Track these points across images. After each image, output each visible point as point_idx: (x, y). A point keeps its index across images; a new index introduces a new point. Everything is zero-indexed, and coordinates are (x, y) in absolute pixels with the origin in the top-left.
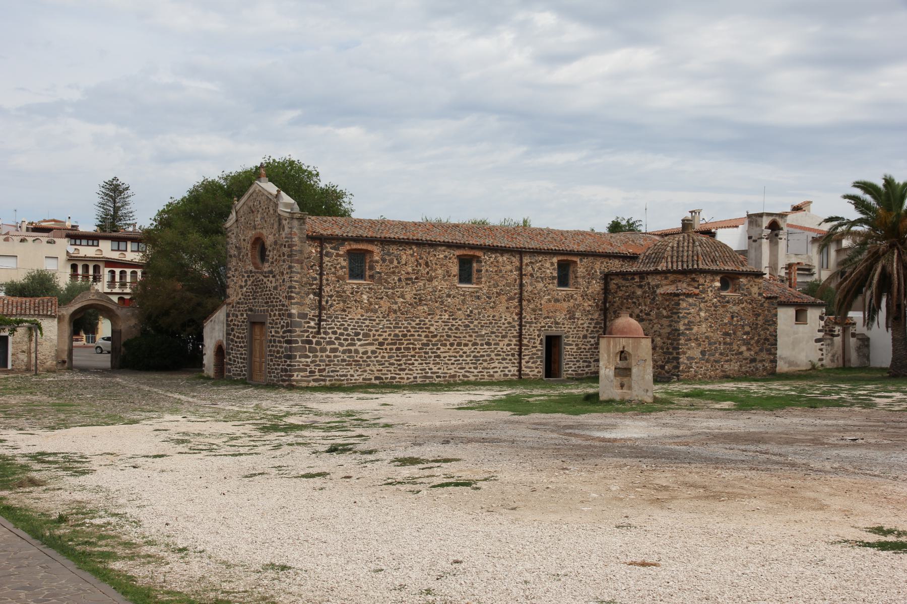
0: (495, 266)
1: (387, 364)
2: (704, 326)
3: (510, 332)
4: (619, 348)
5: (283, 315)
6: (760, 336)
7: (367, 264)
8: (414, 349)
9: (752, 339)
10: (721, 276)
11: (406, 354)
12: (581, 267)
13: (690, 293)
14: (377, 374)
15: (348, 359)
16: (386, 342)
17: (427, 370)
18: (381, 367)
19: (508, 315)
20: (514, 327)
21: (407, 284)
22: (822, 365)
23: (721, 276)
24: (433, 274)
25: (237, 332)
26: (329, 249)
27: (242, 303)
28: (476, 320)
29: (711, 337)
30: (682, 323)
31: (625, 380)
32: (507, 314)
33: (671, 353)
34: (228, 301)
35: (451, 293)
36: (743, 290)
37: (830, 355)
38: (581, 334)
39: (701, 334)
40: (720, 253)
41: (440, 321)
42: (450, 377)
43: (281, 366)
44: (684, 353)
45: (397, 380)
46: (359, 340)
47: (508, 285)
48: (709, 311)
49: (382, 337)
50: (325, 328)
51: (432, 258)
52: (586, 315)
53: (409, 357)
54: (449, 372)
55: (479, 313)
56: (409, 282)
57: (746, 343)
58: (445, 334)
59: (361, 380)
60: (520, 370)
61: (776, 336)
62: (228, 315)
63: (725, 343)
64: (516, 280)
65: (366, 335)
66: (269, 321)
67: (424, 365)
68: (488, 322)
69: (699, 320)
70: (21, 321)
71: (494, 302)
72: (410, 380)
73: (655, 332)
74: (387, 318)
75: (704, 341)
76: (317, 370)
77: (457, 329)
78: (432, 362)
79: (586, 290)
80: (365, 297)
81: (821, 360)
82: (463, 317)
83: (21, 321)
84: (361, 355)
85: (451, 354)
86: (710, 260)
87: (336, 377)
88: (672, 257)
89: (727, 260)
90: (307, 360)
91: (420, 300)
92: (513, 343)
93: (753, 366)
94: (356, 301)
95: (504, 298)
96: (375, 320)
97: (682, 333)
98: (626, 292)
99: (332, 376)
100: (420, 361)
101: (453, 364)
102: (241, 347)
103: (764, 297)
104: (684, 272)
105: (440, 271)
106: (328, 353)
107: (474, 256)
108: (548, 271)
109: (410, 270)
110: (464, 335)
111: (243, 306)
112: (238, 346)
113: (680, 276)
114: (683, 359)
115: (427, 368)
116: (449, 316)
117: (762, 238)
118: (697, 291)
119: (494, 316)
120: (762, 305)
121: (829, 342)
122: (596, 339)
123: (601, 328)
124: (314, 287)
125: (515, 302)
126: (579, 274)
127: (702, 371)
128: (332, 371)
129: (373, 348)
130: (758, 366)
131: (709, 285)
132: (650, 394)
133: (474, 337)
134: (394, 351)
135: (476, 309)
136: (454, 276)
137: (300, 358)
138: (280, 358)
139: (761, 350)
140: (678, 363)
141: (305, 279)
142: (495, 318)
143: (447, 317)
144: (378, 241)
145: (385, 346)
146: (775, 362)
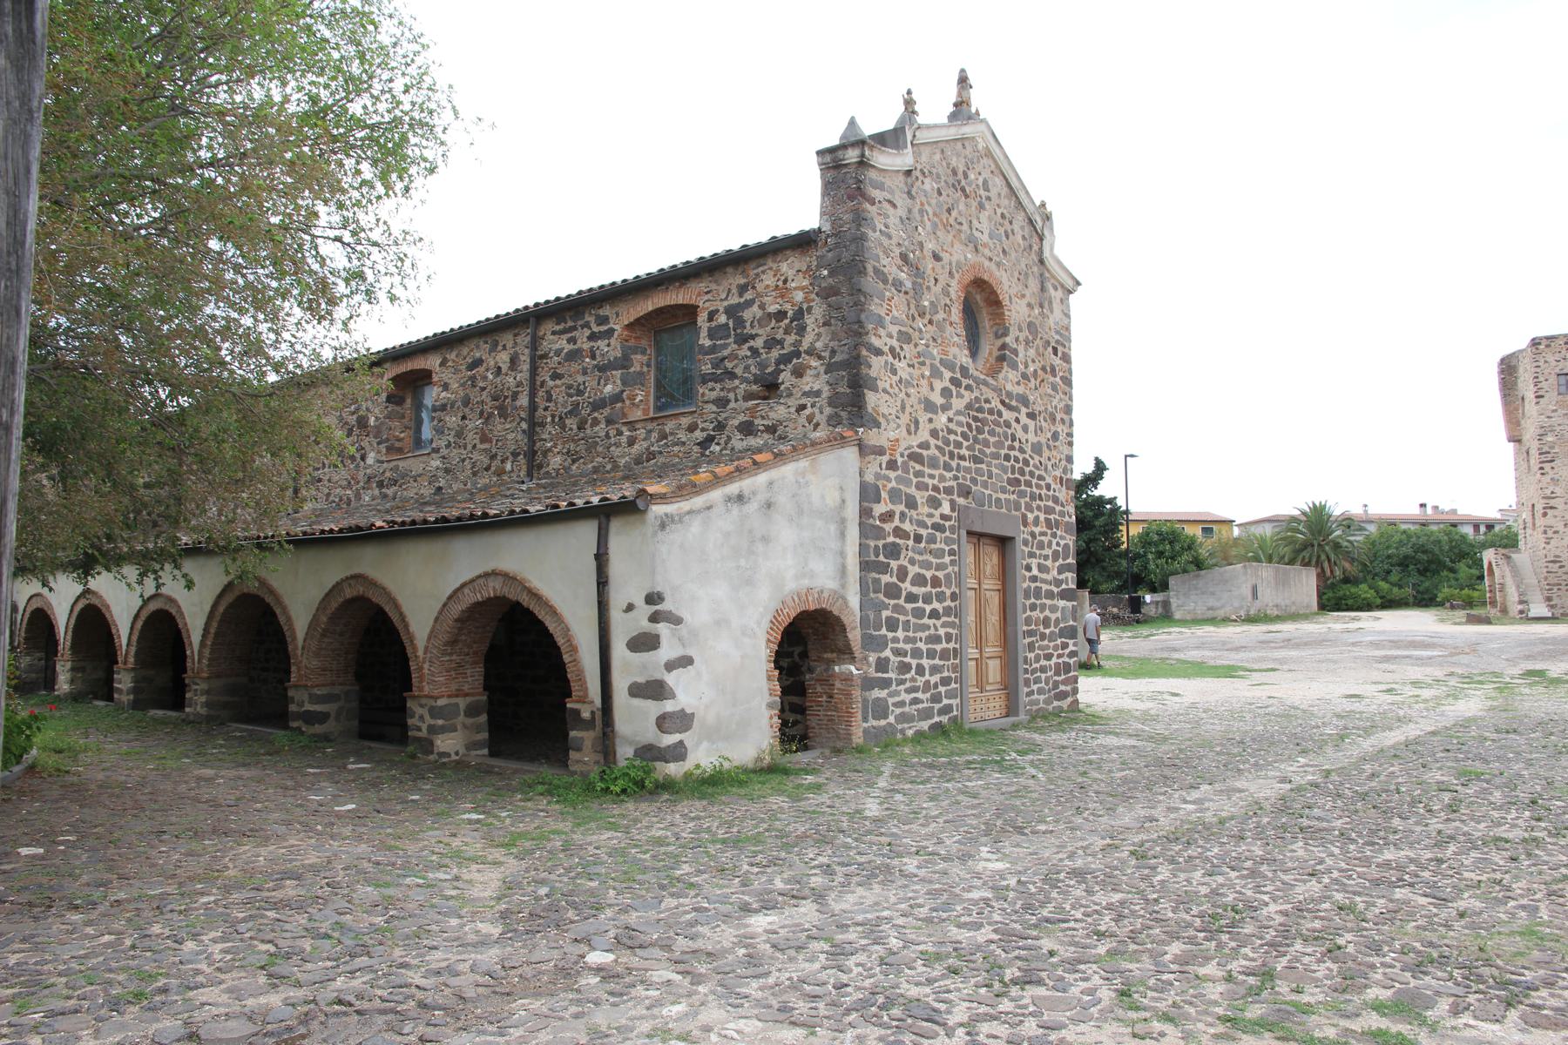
27: (933, 463)
34: (873, 437)
43: (1054, 660)
62: (869, 494)
102: (934, 614)
111: (936, 473)
112: (919, 613)
138: (1052, 637)
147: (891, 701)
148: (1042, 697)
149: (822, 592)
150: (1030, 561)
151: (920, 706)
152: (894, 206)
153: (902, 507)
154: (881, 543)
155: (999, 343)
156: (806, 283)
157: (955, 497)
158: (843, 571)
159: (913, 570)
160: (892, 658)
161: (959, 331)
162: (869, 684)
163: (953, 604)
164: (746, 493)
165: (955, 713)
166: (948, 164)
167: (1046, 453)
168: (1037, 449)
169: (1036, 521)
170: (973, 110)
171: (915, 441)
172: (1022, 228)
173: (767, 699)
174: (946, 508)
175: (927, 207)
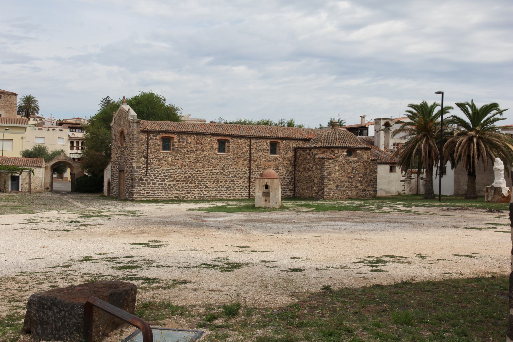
0: (237, 144)
1: (181, 190)
2: (337, 174)
3: (244, 176)
4: (264, 184)
5: (130, 167)
6: (368, 178)
7: (171, 144)
8: (195, 183)
9: (363, 180)
10: (347, 149)
11: (191, 186)
12: (282, 145)
13: (330, 158)
14: (176, 195)
15: (161, 188)
16: (180, 180)
17: (201, 193)
18: (178, 191)
19: (243, 168)
20: (246, 173)
21: (191, 153)
22: (404, 193)
23: (347, 149)
24: (205, 148)
26: (152, 137)
28: (226, 170)
29: (341, 179)
30: (326, 172)
31: (267, 198)
32: (243, 167)
33: (321, 187)
34: (112, 160)
35: (214, 157)
36: (359, 156)
37: (409, 188)
38: (282, 177)
39: (336, 177)
40: (349, 138)
41: (208, 170)
42: (213, 197)
44: (327, 186)
45: (186, 198)
46: (167, 179)
47: (243, 153)
48: (340, 166)
49: (178, 178)
50: (150, 173)
51: (204, 141)
52: (285, 168)
53: (192, 187)
54: (212, 194)
55: (228, 167)
56: (192, 152)
57: (360, 182)
58: (210, 177)
59: (168, 198)
60: (249, 194)
61: (377, 179)
63: (349, 182)
64: (247, 151)
65: (170, 177)
67: (200, 191)
68: (233, 171)
69: (335, 171)
70: (24, 169)
71: (236, 162)
72: (193, 198)
73: (315, 176)
74: (181, 169)
75: (337, 181)
76: (145, 193)
77: (217, 174)
78: (204, 190)
79: (285, 156)
80: (170, 159)
81: (404, 190)
82: (220, 168)
83: (24, 169)
84: (168, 186)
85: (214, 186)
86: (342, 142)
87: (155, 196)
88: (324, 140)
89: (352, 142)
90: (141, 188)
91: (198, 160)
92: (246, 181)
93: (364, 193)
94: (165, 161)
95: (241, 160)
96: (175, 170)
97: (326, 177)
98: (303, 157)
99: (153, 196)
100: (198, 189)
101: (214, 191)
102: (116, 182)
103: (370, 160)
104: (328, 148)
105: (208, 147)
106: (151, 185)
107: (226, 140)
108: (265, 147)
109: (193, 146)
110: (220, 177)
112: (115, 181)
113: (327, 150)
114: (326, 189)
115: (201, 192)
116: (213, 168)
117: (380, 131)
118: (334, 157)
119: (236, 168)
120: (369, 164)
121: (408, 182)
122: (290, 180)
123: (292, 174)
124: (144, 154)
125: (247, 162)
126: (281, 148)
127: (336, 195)
128: (153, 193)
129: (174, 183)
130: (367, 193)
131: (341, 154)
132: (278, 204)
133: (225, 178)
134: (185, 184)
135: (227, 165)
136: (216, 149)
137: (137, 187)
138: (129, 187)
139: (368, 186)
140: (324, 191)
141: (140, 151)
142: (237, 169)
143: (212, 168)
144: (176, 133)
145: (180, 182)
146: (376, 191)
167: (129, 155)
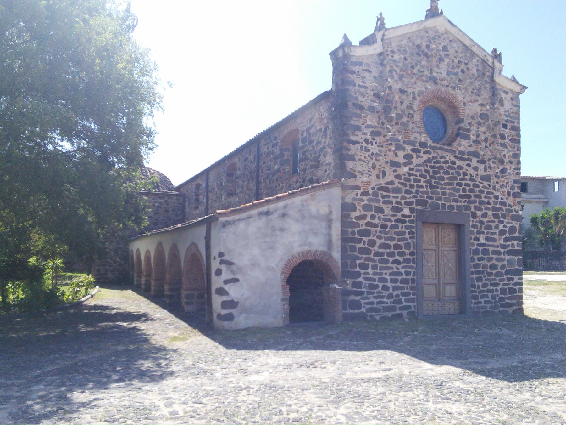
25: (380, 238)
27: (396, 191)
43: (501, 286)
62: (347, 208)
66: (471, 223)
111: (399, 195)
147: (362, 302)
148: (489, 306)
149: (316, 251)
150: (478, 236)
151: (385, 305)
152: (370, 72)
153: (373, 213)
154: (356, 230)
155: (457, 127)
156: (327, 115)
157: (414, 206)
158: (330, 243)
159: (379, 242)
160: (364, 282)
161: (420, 125)
162: (346, 293)
163: (411, 258)
164: (271, 211)
165: (413, 310)
166: (413, 44)
168: (487, 178)
169: (485, 215)
170: (440, 11)
171: (382, 182)
172: (477, 66)
173: (281, 296)
174: (406, 211)
175: (395, 68)
